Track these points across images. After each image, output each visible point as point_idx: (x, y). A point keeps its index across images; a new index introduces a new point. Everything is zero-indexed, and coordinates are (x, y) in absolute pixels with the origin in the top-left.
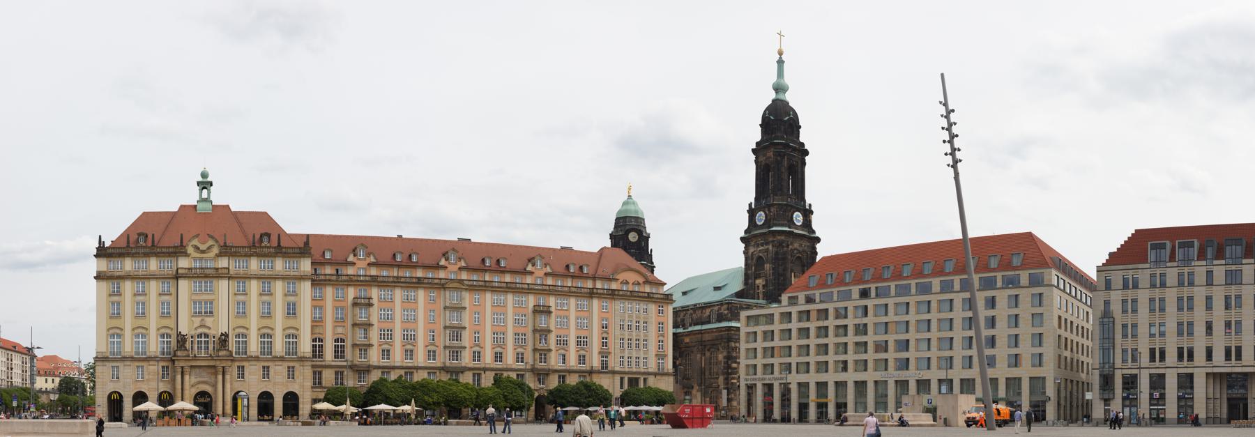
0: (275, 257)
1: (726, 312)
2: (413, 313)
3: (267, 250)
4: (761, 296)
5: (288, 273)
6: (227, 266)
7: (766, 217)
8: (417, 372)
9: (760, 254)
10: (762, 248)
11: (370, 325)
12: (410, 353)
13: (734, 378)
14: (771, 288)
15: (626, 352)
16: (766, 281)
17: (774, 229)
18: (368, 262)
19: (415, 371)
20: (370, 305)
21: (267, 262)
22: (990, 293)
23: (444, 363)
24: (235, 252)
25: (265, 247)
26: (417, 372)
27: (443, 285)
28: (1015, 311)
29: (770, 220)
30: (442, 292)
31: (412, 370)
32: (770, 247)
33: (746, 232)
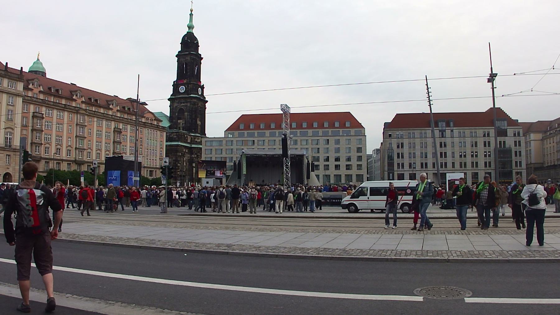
1: (175, 137)
4: (181, 129)
7: (186, 89)
9: (182, 107)
10: (184, 104)
12: (58, 150)
13: (178, 172)
14: (188, 125)
15: (149, 156)
16: (185, 121)
17: (192, 95)
22: (337, 138)
23: (76, 158)
28: (327, 146)
29: (188, 91)
32: (189, 104)
33: (171, 96)
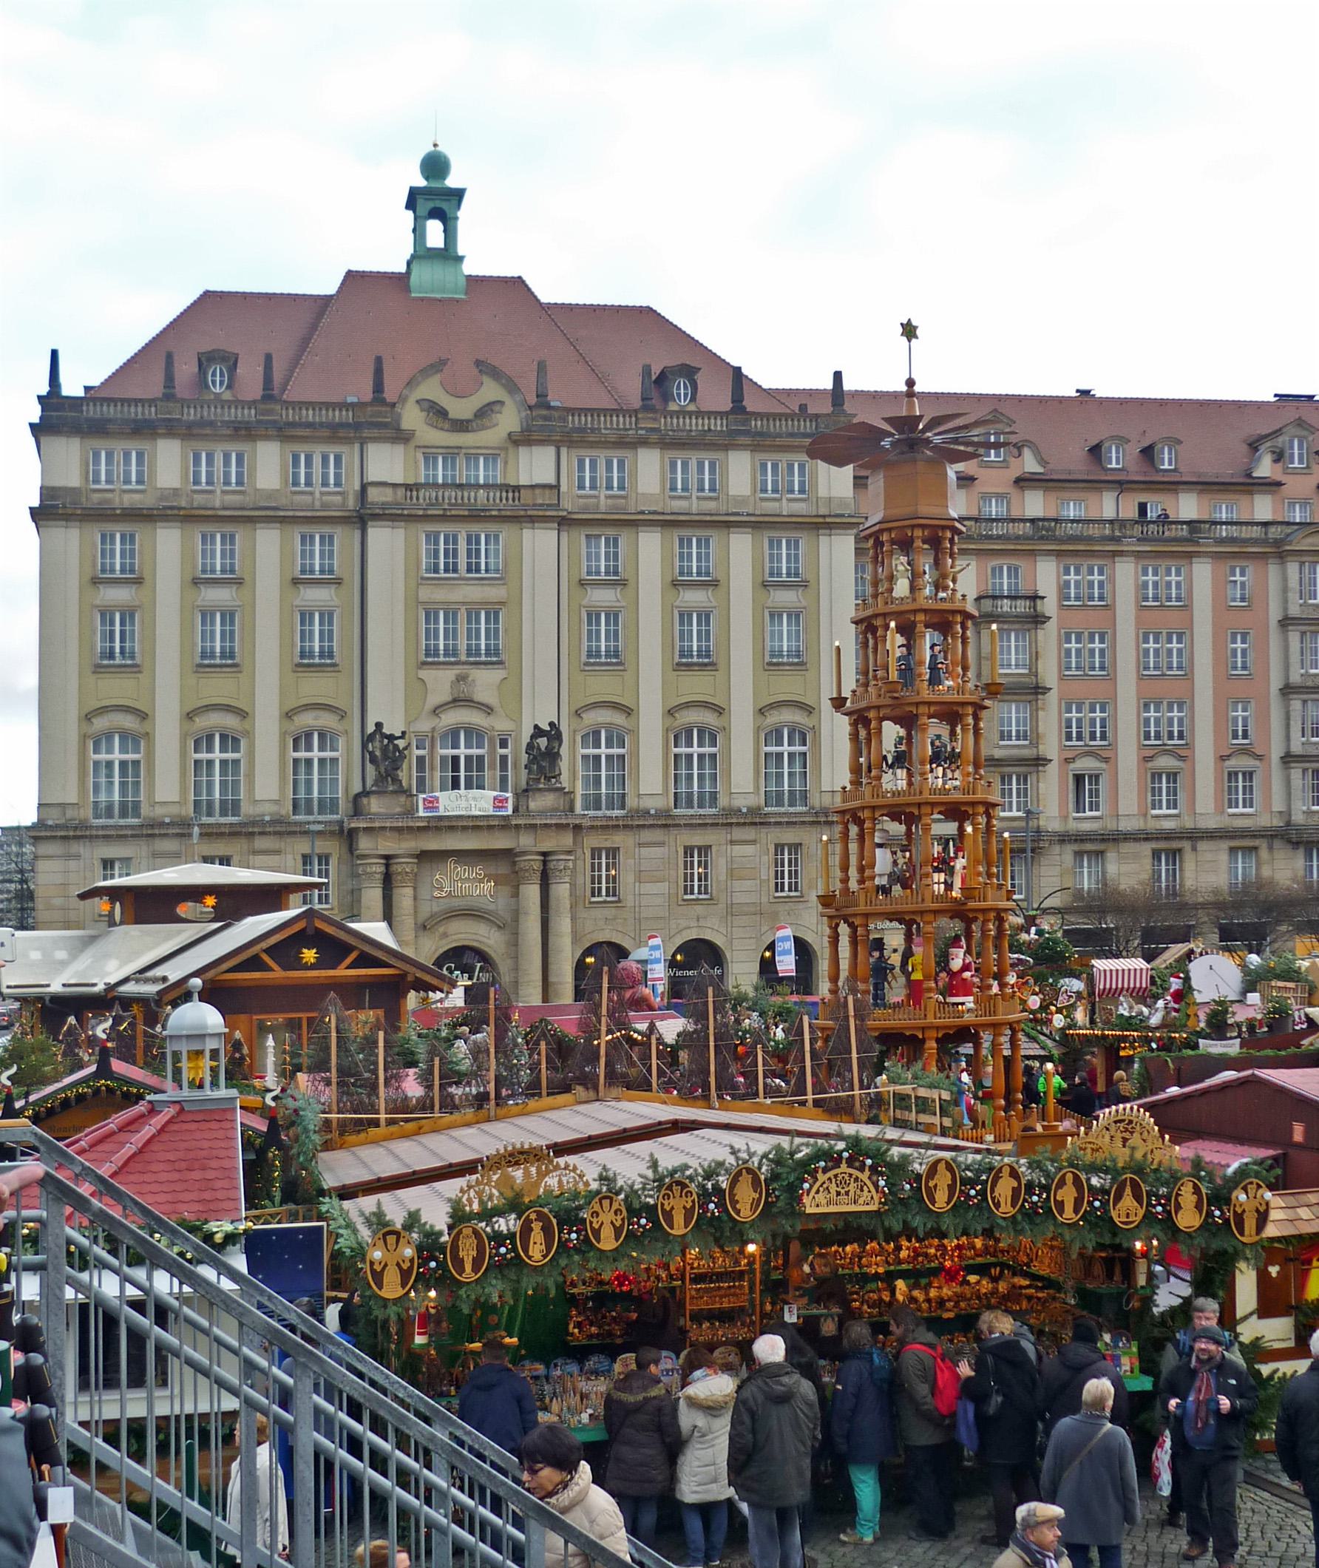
0: (726, 448)
2: (1175, 645)
3: (695, 425)
5: (771, 507)
6: (552, 481)
8: (1194, 849)
11: (1038, 690)
18: (1014, 473)
19: (1186, 845)
20: (1038, 620)
21: (694, 465)
24: (581, 430)
25: (682, 413)
26: (1194, 849)
27: (1278, 543)
30: (1273, 570)
31: (1175, 845)
